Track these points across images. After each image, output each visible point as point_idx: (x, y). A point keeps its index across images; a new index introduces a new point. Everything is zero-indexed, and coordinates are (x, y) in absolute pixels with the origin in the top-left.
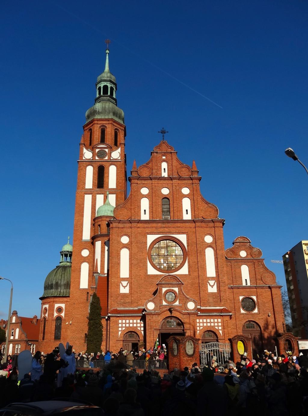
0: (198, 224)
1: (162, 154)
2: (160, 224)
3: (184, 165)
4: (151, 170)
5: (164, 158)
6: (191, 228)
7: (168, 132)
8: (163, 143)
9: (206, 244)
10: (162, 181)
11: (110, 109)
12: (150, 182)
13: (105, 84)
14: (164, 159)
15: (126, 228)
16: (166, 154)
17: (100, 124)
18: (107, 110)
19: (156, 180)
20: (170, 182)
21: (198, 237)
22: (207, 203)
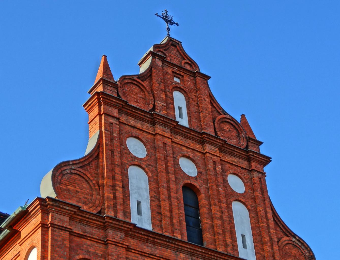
3: (228, 117)
5: (176, 80)
8: (172, 45)
14: (176, 83)
15: (91, 239)
16: (182, 74)
19: (167, 130)
22: (288, 234)
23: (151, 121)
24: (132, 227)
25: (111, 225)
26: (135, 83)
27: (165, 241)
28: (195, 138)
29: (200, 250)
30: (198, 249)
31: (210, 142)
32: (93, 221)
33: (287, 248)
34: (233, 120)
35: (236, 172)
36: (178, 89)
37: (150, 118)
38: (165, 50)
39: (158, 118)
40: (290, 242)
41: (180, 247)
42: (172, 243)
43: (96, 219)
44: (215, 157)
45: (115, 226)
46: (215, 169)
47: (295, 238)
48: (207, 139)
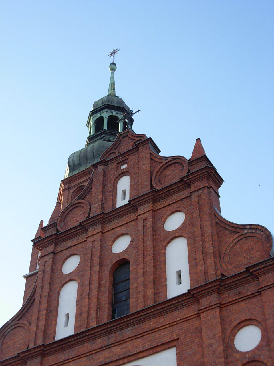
0: (205, 302)
1: (116, 163)
2: (99, 341)
3: (169, 159)
4: (89, 207)
5: (124, 167)
6: (187, 320)
7: (138, 111)
8: (124, 137)
9: (238, 356)
10: (112, 223)
11: (94, 151)
12: (82, 238)
13: (98, 115)
16: (127, 157)
17: (74, 186)
18: (89, 156)
20: (133, 216)
21: (208, 341)
22: (237, 230)
23: (84, 230)
24: (42, 348)
25: (26, 357)
26: (76, 206)
27: (77, 339)
28: (128, 211)
29: (112, 325)
30: (109, 326)
31: (140, 203)
32: (15, 363)
33: (238, 246)
34: (175, 158)
35: (174, 210)
36: (123, 175)
37: (82, 228)
38: (115, 149)
39: (86, 224)
40: (241, 237)
41: (93, 335)
42: (84, 337)
43: (15, 360)
44: (147, 214)
45: (29, 356)
46: (144, 226)
47: (246, 229)
48: (136, 204)
